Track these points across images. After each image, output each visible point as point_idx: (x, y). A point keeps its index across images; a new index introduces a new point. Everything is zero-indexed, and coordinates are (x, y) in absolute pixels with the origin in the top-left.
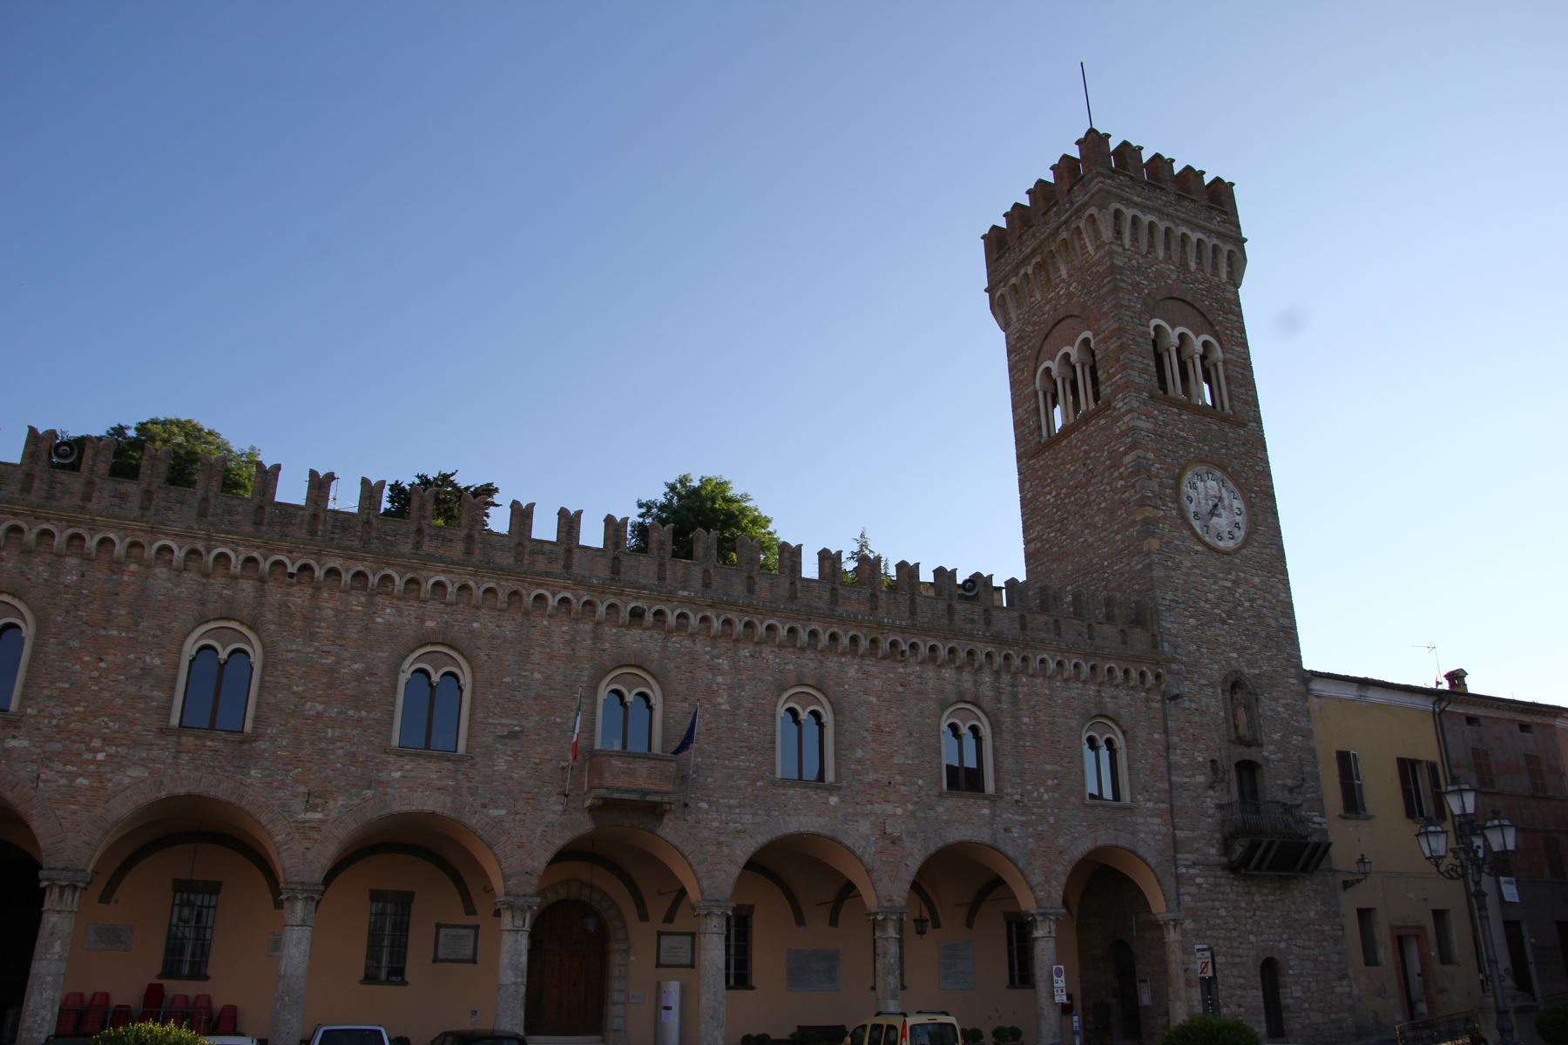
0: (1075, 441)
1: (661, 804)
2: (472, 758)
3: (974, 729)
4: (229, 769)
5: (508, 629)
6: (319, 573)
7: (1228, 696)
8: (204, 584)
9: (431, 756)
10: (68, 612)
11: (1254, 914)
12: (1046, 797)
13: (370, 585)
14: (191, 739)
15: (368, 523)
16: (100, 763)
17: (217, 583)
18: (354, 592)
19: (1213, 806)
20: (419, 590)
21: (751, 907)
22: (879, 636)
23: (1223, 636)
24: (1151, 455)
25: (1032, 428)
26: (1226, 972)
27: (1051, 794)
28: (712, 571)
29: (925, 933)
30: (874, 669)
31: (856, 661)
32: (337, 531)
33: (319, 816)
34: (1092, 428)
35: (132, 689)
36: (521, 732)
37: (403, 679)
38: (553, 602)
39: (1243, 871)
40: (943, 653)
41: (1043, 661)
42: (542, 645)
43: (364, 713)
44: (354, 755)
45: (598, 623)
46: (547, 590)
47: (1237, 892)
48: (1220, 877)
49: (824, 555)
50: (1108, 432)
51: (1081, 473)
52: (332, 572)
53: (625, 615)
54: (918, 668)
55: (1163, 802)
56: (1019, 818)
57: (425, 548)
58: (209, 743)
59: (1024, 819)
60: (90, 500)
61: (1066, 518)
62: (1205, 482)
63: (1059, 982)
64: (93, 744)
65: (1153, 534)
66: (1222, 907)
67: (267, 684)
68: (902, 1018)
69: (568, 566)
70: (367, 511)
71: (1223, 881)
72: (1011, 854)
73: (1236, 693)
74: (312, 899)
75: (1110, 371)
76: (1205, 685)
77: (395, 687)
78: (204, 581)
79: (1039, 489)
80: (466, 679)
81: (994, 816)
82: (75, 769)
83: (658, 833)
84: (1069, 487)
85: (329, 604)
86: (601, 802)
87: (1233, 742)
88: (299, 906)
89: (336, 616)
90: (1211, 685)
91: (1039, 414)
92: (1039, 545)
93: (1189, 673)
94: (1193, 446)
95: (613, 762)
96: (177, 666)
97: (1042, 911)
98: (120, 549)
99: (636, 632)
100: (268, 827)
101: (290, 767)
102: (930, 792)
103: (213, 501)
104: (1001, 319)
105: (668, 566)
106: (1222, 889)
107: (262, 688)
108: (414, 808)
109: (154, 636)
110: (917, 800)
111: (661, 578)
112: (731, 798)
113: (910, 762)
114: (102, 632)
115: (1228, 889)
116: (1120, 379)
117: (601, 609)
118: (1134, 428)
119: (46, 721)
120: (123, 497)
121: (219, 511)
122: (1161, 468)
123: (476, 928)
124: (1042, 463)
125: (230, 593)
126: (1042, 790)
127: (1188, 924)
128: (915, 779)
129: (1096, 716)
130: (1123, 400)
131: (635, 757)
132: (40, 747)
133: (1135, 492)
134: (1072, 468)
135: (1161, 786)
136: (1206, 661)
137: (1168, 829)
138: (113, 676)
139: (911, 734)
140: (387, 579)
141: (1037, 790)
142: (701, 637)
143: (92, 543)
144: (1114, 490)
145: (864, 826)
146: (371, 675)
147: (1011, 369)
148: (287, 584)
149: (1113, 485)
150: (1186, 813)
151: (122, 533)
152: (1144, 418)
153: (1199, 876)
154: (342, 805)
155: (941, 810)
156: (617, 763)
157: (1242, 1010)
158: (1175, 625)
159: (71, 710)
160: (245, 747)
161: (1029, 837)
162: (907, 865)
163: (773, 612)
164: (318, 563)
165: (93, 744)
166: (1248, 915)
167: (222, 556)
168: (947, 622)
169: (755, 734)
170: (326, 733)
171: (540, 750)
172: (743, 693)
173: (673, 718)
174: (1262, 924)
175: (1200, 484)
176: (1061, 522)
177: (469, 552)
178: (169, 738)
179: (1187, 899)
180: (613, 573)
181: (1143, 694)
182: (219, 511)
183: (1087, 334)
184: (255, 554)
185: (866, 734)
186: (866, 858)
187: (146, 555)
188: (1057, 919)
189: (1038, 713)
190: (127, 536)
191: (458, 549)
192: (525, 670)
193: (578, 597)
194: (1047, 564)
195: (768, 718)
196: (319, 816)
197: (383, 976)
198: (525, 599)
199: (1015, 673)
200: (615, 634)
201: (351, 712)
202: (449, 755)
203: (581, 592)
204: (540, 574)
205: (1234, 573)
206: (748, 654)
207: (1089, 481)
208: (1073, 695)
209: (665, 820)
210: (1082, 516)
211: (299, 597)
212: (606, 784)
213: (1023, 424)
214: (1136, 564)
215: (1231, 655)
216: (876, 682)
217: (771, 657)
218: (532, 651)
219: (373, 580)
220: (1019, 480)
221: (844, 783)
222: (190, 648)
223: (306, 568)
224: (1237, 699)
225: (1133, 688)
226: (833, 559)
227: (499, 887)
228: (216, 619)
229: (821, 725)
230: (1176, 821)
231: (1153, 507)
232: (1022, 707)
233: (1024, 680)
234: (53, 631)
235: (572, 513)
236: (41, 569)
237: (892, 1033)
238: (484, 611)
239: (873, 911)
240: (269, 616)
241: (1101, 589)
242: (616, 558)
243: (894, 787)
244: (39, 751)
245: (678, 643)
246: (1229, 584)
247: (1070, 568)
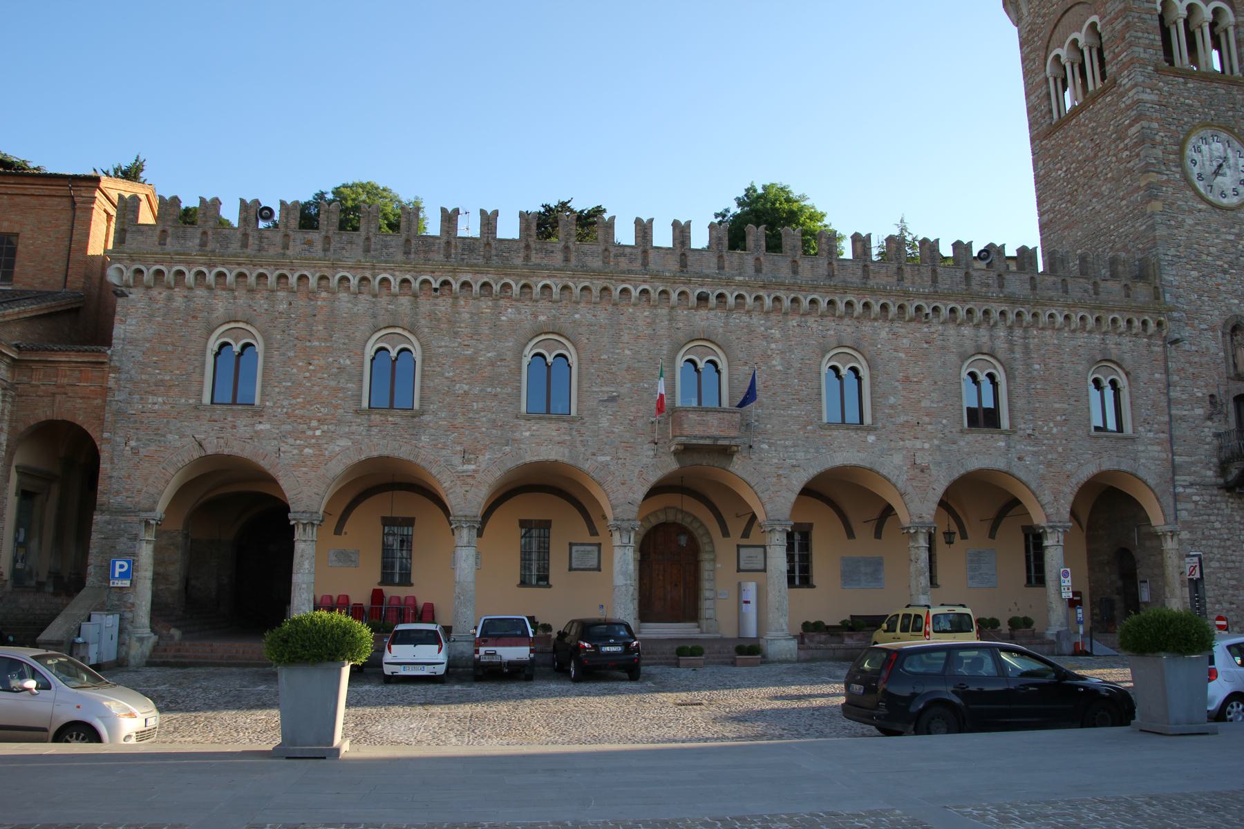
0: (1083, 120)
1: (729, 447)
2: (582, 418)
3: (991, 377)
4: (406, 436)
5: (603, 317)
6: (456, 286)
7: (1228, 338)
8: (374, 303)
9: (551, 419)
10: (284, 331)
12: (1055, 430)
13: (494, 291)
14: (378, 416)
15: (488, 244)
16: (318, 438)
17: (384, 300)
18: (483, 298)
19: (1211, 435)
20: (532, 293)
21: (811, 525)
22: (906, 303)
23: (1224, 285)
24: (1155, 125)
25: (1043, 113)
26: (1220, 575)
27: (1059, 428)
28: (761, 258)
29: (952, 543)
30: (903, 330)
31: (887, 325)
32: (465, 253)
33: (473, 467)
34: (1099, 106)
35: (333, 383)
36: (618, 396)
37: (526, 362)
38: (635, 293)
39: (1237, 490)
40: (962, 313)
41: (1051, 316)
42: (630, 328)
43: (499, 390)
44: (494, 421)
45: (672, 308)
46: (630, 284)
47: (1232, 508)
48: (1216, 496)
49: (856, 238)
50: (1113, 109)
51: (1088, 148)
52: (466, 285)
53: (693, 299)
54: (940, 328)
55: (1163, 432)
56: (1031, 449)
57: (533, 259)
58: (390, 419)
59: (1035, 449)
60: (288, 249)
61: (1076, 190)
62: (1210, 144)
64: (312, 425)
65: (1156, 198)
67: (427, 373)
68: (926, 609)
69: (645, 264)
70: (486, 235)
71: (1219, 499)
72: (1024, 478)
73: (1236, 335)
74: (474, 527)
75: (1116, 51)
76: (1206, 330)
77: (520, 369)
78: (374, 300)
79: (1051, 166)
80: (573, 359)
81: (1008, 447)
82: (302, 442)
83: (730, 469)
84: (1078, 162)
85: (466, 309)
86: (683, 447)
87: (1232, 379)
88: (465, 532)
89: (471, 318)
90: (1212, 329)
91: (1049, 99)
92: (1052, 215)
93: (1189, 320)
94: (1198, 112)
95: (690, 416)
96: (362, 365)
97: (1051, 524)
98: (313, 282)
99: (703, 312)
100: (438, 477)
101: (449, 433)
102: (953, 430)
103: (373, 240)
104: (1013, 16)
105: (726, 257)
106: (1218, 505)
107: (423, 376)
108: (541, 458)
109: (344, 344)
110: (943, 436)
111: (721, 268)
112: (788, 440)
113: (935, 406)
114: (308, 344)
115: (1223, 505)
116: (1125, 57)
117: (674, 296)
118: (1139, 101)
119: (279, 410)
120: (310, 243)
121: (379, 247)
122: (1166, 136)
123: (599, 545)
124: (1053, 142)
125: (393, 307)
126: (1051, 425)
127: (1185, 535)
128: (940, 420)
129: (1100, 361)
130: (1128, 76)
131: (707, 411)
132: (278, 429)
133: (1140, 160)
134: (1081, 145)
135: (1162, 419)
136: (1207, 308)
137: (1168, 456)
138: (319, 375)
139: (935, 383)
140: (506, 286)
141: (1047, 425)
142: (757, 313)
143: (293, 280)
144: (1119, 161)
145: (897, 459)
146: (502, 360)
147: (1023, 60)
148: (434, 297)
149: (1119, 156)
150: (1185, 441)
151: (312, 270)
152: (1148, 90)
153: (1196, 494)
154: (489, 459)
155: (962, 443)
156: (692, 416)
157: (1235, 606)
158: (1177, 278)
159: (294, 402)
160: (416, 420)
161: (1040, 464)
162: (934, 489)
163: (815, 288)
164: (454, 279)
165: (312, 425)
167: (384, 280)
168: (964, 287)
169: (804, 388)
170: (473, 406)
171: (633, 409)
172: (793, 356)
173: (737, 379)
175: (1204, 148)
176: (1071, 194)
177: (567, 260)
178: (363, 417)
179: (1184, 515)
180: (681, 266)
181: (1145, 340)
182: (379, 247)
183: (1095, 18)
184: (408, 277)
185: (897, 384)
186: (900, 484)
187: (331, 285)
188: (1065, 531)
189: (1047, 360)
190: (316, 272)
191: (558, 258)
192: (618, 349)
193: (654, 288)
194: (1059, 232)
195: (814, 375)
196: (473, 467)
197: (534, 582)
198: (613, 293)
199: (1026, 327)
200: (687, 315)
201: (489, 390)
202: (565, 417)
203: (657, 284)
204: (624, 272)
205: (1237, 227)
206: (795, 324)
207: (1096, 155)
209: (735, 459)
210: (1090, 187)
211: (443, 305)
212: (686, 433)
213: (1035, 109)
214: (1141, 226)
215: (1232, 301)
216: (905, 341)
217: (815, 325)
218: (622, 333)
219: (496, 288)
220: (1033, 160)
221: (880, 425)
222: (370, 351)
223: (445, 283)
224: (1237, 341)
225: (1136, 335)
226: (863, 241)
227: (610, 516)
228: (385, 328)
229: (859, 379)
230: (1175, 448)
231: (1157, 172)
232: (1033, 356)
233: (1035, 332)
234: (276, 346)
235: (645, 221)
236: (262, 302)
237: (919, 620)
238: (582, 305)
239: (907, 525)
240: (423, 322)
241: (1107, 250)
242: (683, 254)
244: (277, 431)
245: (738, 319)
246: (1232, 237)
247: (1079, 234)
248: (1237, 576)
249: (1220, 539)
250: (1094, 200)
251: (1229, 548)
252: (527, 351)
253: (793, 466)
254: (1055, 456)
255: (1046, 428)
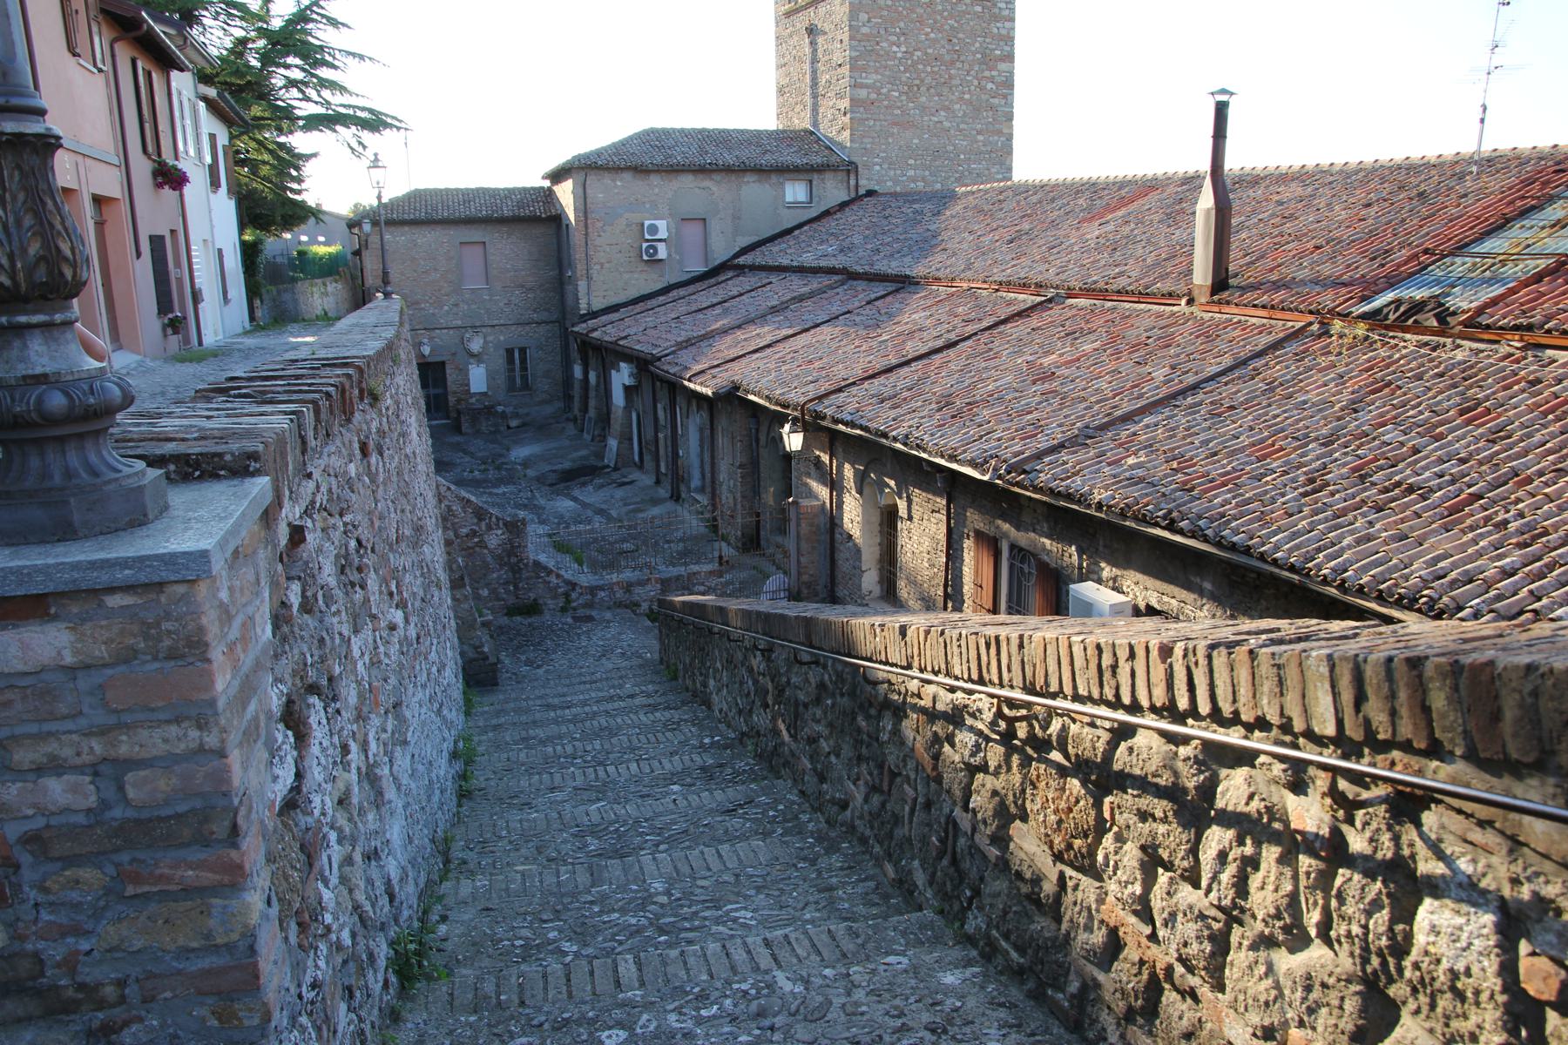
84: (926, 53)
92: (874, 96)
134: (932, 35)
144: (982, 89)
247: (916, 141)
250: (943, 113)
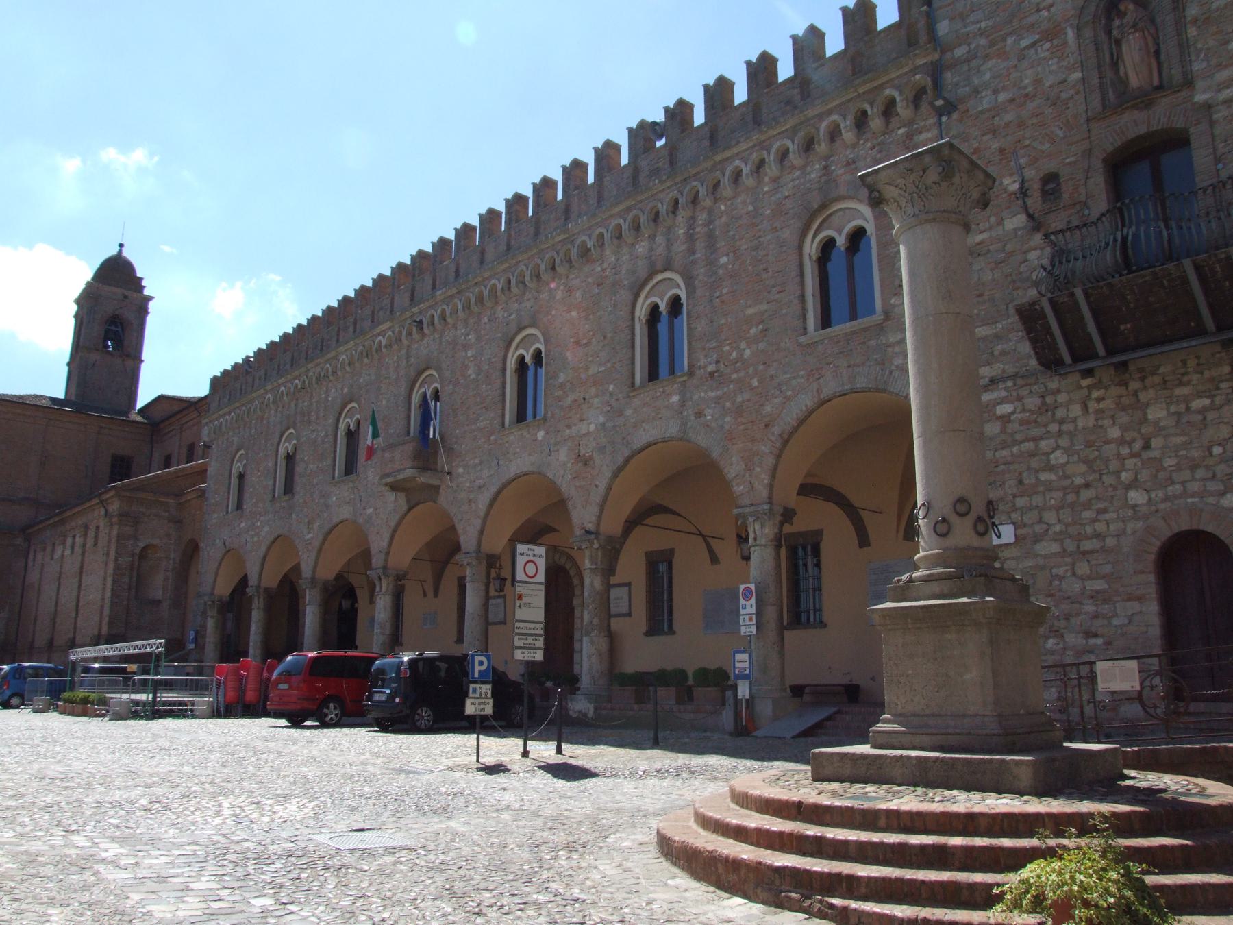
11: (1147, 447)
26: (1061, 571)
48: (1059, 391)
59: (719, 393)
63: (748, 607)
66: (1058, 447)
71: (1062, 398)
81: (683, 403)
106: (1060, 413)
115: (1076, 410)
126: (743, 345)
153: (1003, 401)
157: (1099, 641)
162: (596, 486)
166: (1125, 451)
174: (1169, 462)
208: (787, 194)
209: (441, 491)
243: (589, 402)
248: (1107, 569)
249: (1065, 488)
251: (1087, 506)
252: (340, 425)
253: (480, 487)
254: (747, 396)
255: (734, 354)
